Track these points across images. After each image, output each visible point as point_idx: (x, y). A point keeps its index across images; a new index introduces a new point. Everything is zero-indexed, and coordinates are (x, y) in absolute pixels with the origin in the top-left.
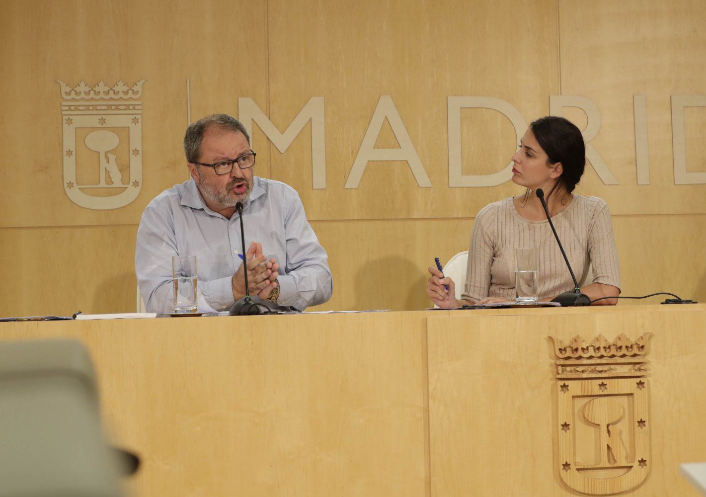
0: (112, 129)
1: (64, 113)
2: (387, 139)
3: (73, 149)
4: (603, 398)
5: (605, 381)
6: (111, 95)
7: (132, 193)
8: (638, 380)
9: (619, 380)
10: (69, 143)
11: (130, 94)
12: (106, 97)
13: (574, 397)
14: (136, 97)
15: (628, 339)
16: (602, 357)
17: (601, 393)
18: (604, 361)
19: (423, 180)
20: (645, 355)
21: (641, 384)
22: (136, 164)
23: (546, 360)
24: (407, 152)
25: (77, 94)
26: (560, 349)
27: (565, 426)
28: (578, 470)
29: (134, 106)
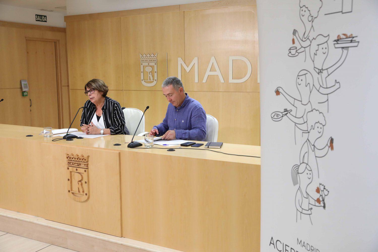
0: (150, 66)
1: (141, 62)
2: (212, 69)
3: (143, 71)
4: (77, 173)
5: (77, 168)
6: (150, 57)
7: (155, 82)
8: (85, 169)
9: (81, 168)
10: (142, 70)
11: (154, 57)
12: (149, 58)
13: (71, 172)
14: (155, 58)
15: (83, 156)
16: (76, 161)
17: (76, 171)
18: (77, 162)
19: (222, 81)
20: (87, 162)
21: (85, 171)
22: (156, 74)
23: (66, 161)
24: (218, 73)
25: (143, 57)
26: (67, 158)
27: (69, 180)
28: (73, 193)
29: (155, 60)
